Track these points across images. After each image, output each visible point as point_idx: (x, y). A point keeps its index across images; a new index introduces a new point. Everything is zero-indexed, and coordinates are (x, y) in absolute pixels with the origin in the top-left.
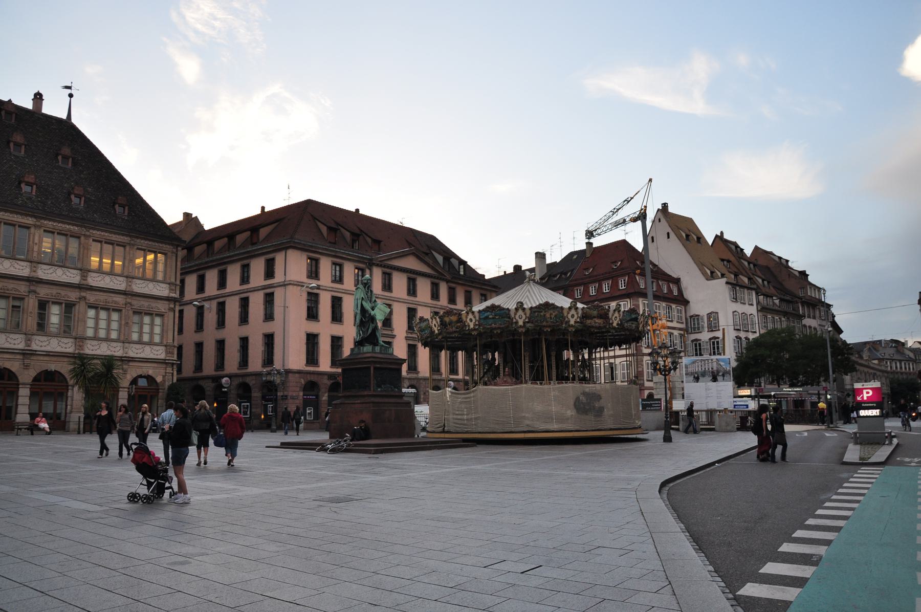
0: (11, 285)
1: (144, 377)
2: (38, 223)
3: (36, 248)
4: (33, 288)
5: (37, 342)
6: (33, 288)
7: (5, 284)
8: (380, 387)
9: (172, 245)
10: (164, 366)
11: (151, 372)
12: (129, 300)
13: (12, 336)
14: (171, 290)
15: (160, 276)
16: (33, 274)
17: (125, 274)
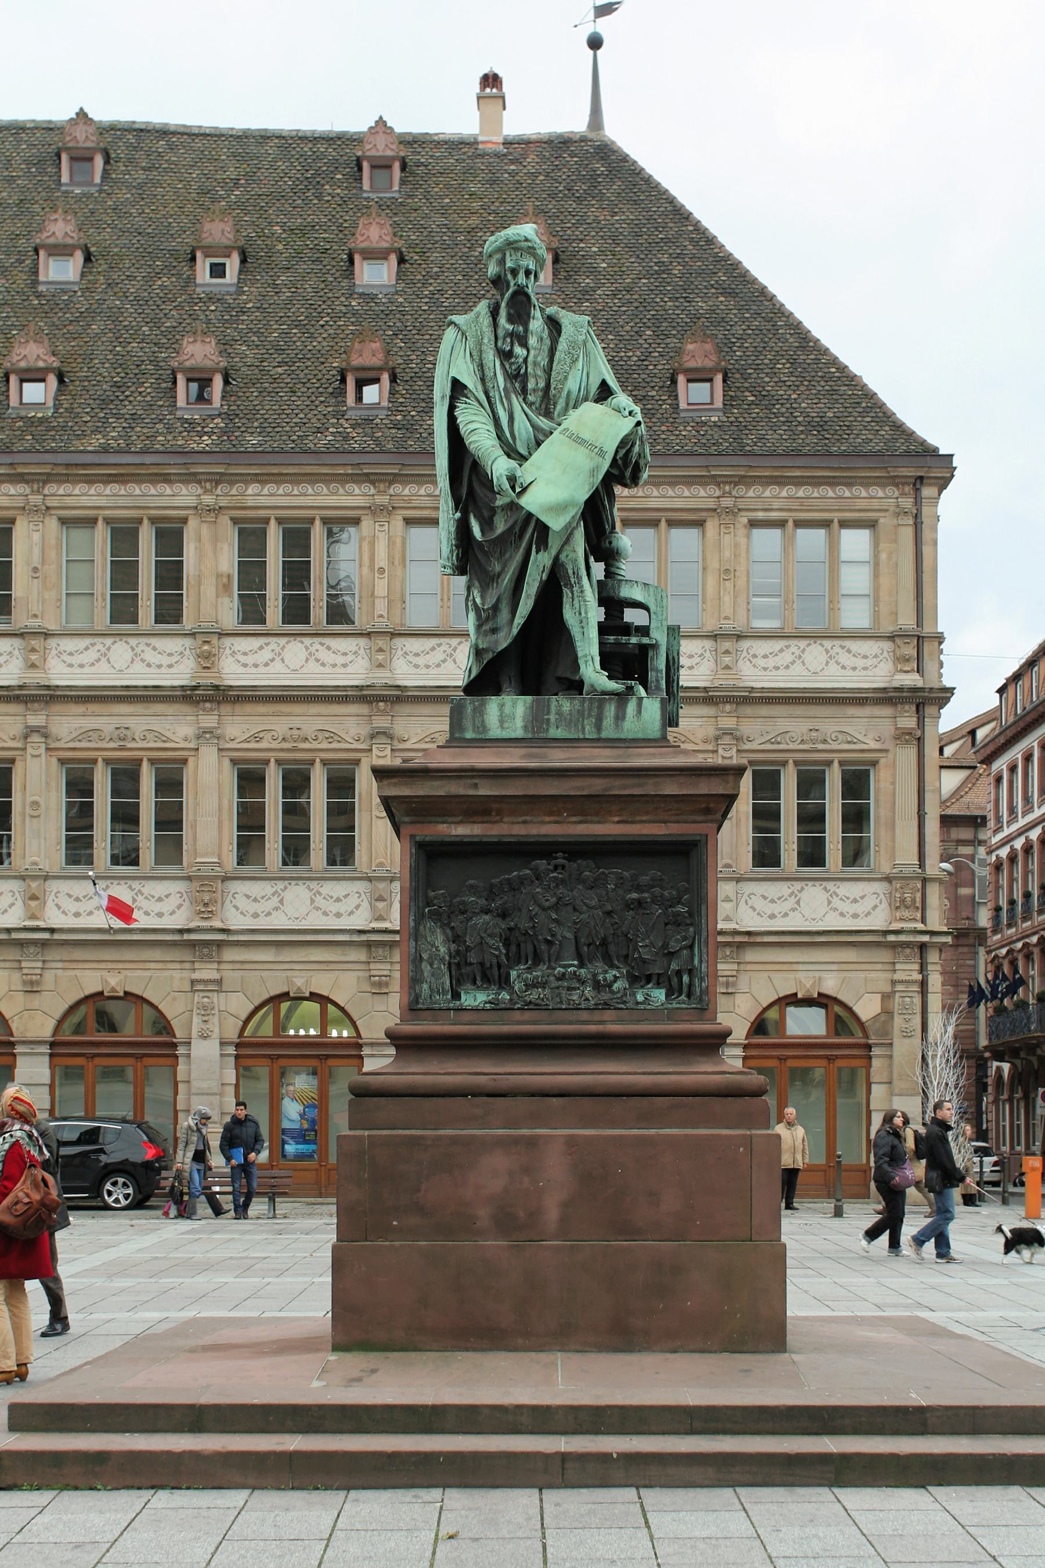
0: (309, 722)
1: (808, 1002)
2: (382, 500)
3: (381, 587)
4: (381, 722)
5: (241, 902)
6: (381, 722)
7: (296, 722)
8: (492, 976)
9: (895, 481)
10: (885, 956)
11: (830, 985)
12: (728, 722)
13: (327, 888)
14: (900, 659)
15: (855, 615)
16: (381, 677)
17: (711, 625)
